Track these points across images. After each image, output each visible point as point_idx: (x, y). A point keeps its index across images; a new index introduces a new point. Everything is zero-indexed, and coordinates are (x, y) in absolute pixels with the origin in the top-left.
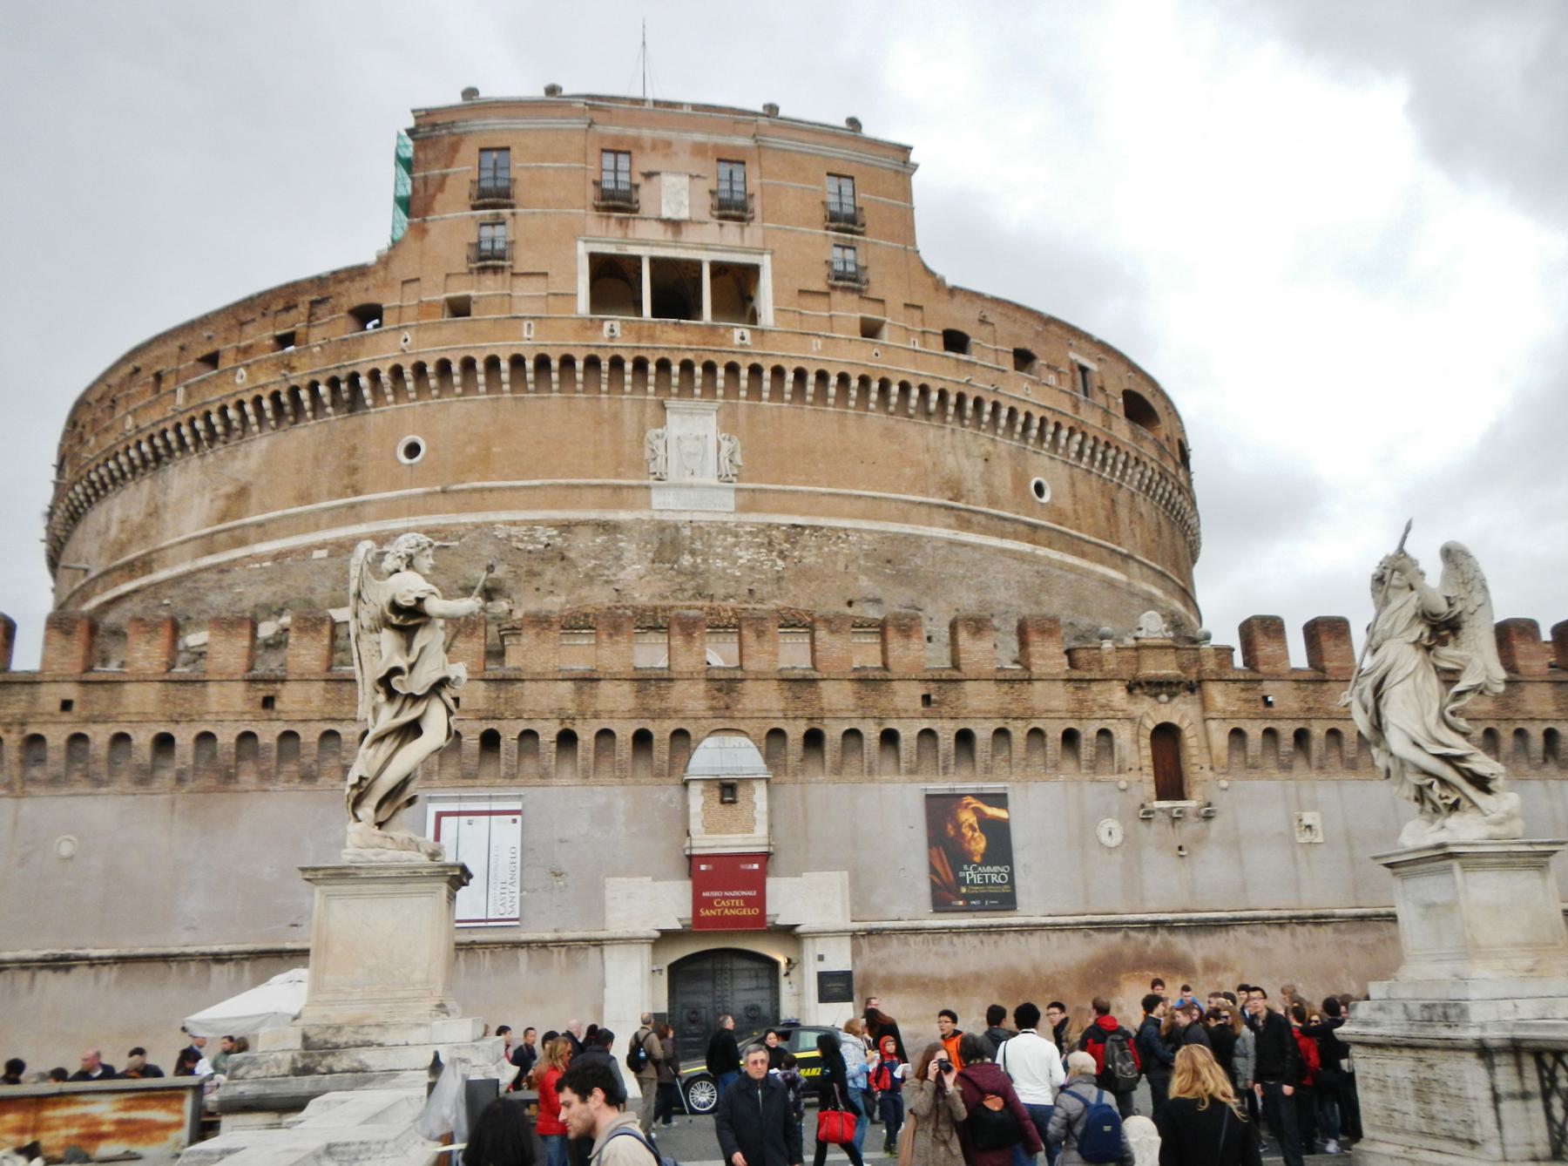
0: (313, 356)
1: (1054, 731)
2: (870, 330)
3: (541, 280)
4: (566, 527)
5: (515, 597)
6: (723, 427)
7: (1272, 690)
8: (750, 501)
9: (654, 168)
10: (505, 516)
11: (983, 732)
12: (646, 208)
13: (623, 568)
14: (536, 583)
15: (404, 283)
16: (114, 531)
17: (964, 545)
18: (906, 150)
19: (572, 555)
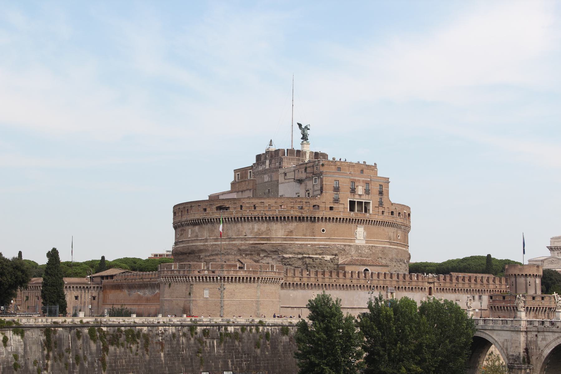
0: (307, 212)
1: (420, 288)
2: (383, 212)
3: (343, 205)
4: (345, 245)
5: (339, 256)
6: (364, 230)
7: (441, 283)
8: (367, 242)
9: (358, 185)
10: (337, 243)
11: (414, 287)
12: (356, 193)
13: (352, 252)
14: (341, 254)
15: (323, 202)
16: (256, 230)
17: (391, 248)
18: (389, 178)
19: (346, 250)
